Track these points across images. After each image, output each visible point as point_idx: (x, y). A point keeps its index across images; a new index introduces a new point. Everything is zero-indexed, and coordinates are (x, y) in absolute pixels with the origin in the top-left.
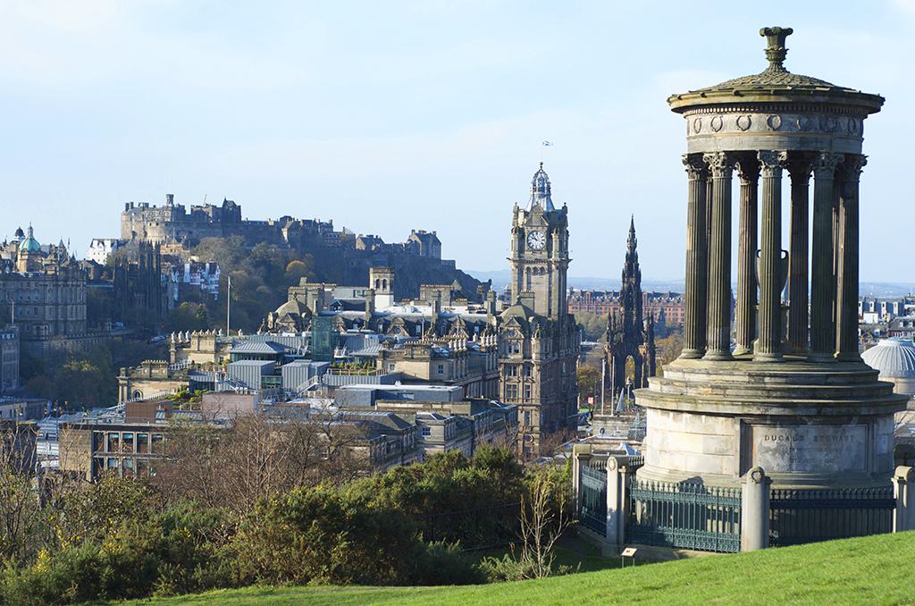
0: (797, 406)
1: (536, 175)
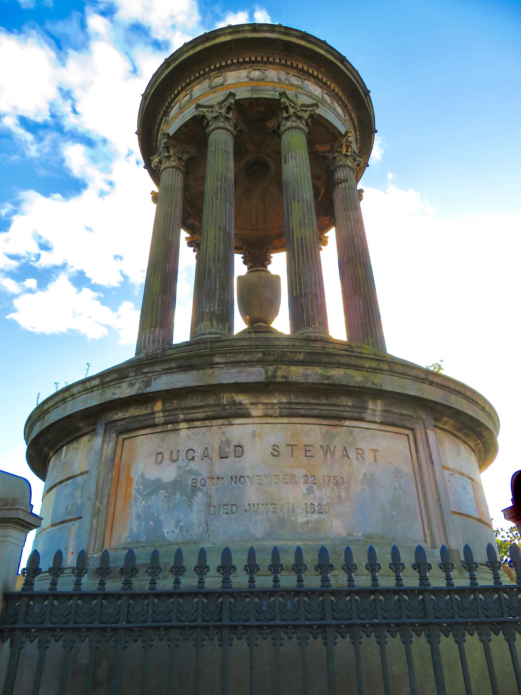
0: (212, 365)
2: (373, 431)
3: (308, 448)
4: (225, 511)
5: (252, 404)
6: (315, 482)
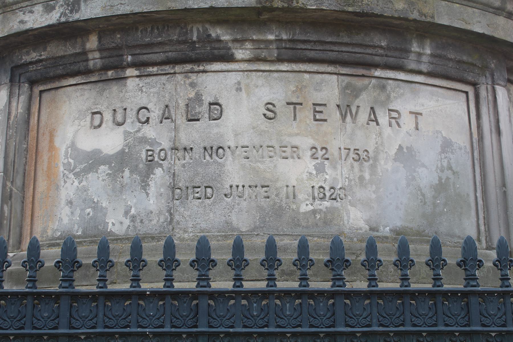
2: (417, 85)
3: (318, 109)
4: (197, 195)
5: (235, 41)
6: (326, 156)
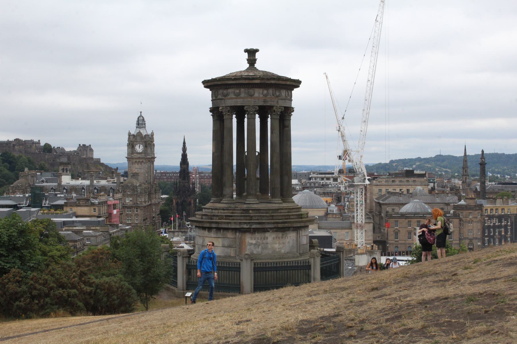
1: (139, 118)
